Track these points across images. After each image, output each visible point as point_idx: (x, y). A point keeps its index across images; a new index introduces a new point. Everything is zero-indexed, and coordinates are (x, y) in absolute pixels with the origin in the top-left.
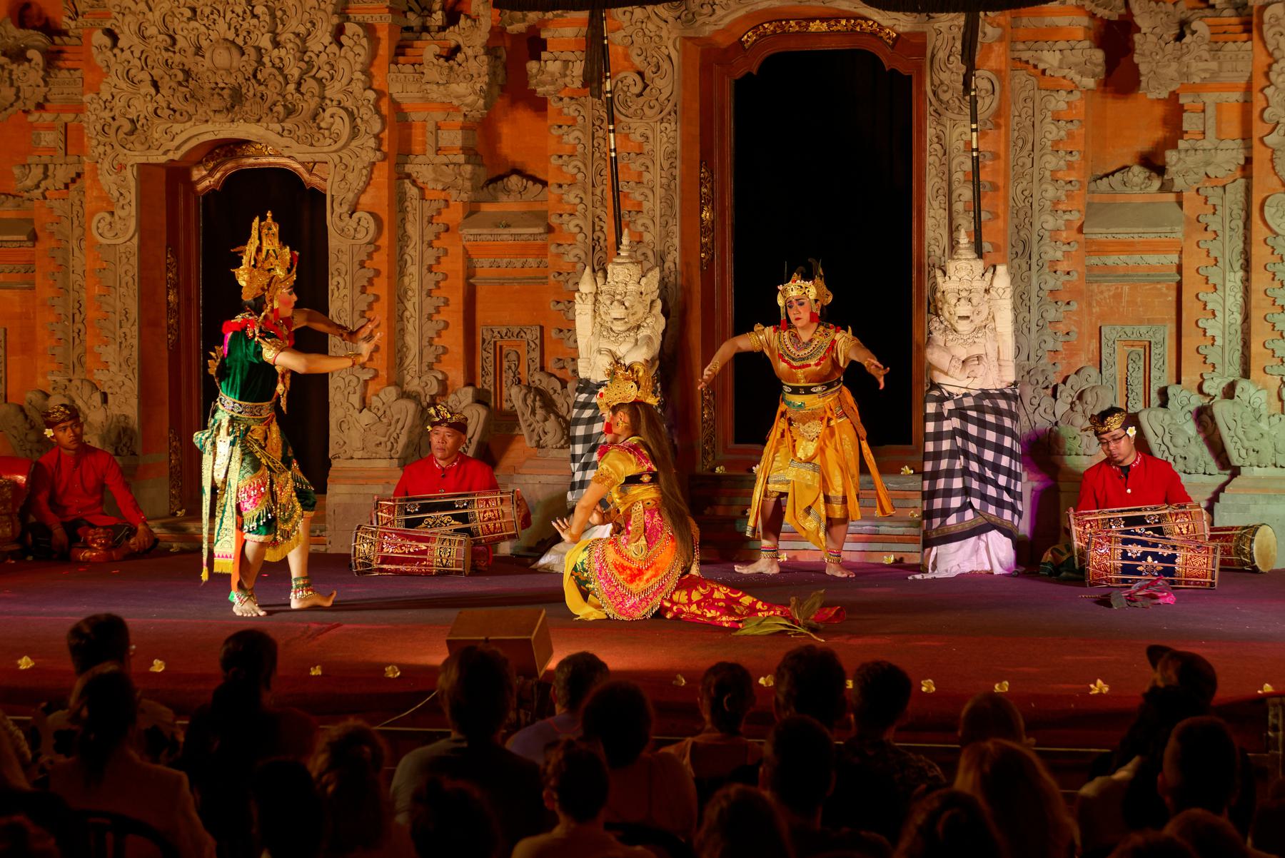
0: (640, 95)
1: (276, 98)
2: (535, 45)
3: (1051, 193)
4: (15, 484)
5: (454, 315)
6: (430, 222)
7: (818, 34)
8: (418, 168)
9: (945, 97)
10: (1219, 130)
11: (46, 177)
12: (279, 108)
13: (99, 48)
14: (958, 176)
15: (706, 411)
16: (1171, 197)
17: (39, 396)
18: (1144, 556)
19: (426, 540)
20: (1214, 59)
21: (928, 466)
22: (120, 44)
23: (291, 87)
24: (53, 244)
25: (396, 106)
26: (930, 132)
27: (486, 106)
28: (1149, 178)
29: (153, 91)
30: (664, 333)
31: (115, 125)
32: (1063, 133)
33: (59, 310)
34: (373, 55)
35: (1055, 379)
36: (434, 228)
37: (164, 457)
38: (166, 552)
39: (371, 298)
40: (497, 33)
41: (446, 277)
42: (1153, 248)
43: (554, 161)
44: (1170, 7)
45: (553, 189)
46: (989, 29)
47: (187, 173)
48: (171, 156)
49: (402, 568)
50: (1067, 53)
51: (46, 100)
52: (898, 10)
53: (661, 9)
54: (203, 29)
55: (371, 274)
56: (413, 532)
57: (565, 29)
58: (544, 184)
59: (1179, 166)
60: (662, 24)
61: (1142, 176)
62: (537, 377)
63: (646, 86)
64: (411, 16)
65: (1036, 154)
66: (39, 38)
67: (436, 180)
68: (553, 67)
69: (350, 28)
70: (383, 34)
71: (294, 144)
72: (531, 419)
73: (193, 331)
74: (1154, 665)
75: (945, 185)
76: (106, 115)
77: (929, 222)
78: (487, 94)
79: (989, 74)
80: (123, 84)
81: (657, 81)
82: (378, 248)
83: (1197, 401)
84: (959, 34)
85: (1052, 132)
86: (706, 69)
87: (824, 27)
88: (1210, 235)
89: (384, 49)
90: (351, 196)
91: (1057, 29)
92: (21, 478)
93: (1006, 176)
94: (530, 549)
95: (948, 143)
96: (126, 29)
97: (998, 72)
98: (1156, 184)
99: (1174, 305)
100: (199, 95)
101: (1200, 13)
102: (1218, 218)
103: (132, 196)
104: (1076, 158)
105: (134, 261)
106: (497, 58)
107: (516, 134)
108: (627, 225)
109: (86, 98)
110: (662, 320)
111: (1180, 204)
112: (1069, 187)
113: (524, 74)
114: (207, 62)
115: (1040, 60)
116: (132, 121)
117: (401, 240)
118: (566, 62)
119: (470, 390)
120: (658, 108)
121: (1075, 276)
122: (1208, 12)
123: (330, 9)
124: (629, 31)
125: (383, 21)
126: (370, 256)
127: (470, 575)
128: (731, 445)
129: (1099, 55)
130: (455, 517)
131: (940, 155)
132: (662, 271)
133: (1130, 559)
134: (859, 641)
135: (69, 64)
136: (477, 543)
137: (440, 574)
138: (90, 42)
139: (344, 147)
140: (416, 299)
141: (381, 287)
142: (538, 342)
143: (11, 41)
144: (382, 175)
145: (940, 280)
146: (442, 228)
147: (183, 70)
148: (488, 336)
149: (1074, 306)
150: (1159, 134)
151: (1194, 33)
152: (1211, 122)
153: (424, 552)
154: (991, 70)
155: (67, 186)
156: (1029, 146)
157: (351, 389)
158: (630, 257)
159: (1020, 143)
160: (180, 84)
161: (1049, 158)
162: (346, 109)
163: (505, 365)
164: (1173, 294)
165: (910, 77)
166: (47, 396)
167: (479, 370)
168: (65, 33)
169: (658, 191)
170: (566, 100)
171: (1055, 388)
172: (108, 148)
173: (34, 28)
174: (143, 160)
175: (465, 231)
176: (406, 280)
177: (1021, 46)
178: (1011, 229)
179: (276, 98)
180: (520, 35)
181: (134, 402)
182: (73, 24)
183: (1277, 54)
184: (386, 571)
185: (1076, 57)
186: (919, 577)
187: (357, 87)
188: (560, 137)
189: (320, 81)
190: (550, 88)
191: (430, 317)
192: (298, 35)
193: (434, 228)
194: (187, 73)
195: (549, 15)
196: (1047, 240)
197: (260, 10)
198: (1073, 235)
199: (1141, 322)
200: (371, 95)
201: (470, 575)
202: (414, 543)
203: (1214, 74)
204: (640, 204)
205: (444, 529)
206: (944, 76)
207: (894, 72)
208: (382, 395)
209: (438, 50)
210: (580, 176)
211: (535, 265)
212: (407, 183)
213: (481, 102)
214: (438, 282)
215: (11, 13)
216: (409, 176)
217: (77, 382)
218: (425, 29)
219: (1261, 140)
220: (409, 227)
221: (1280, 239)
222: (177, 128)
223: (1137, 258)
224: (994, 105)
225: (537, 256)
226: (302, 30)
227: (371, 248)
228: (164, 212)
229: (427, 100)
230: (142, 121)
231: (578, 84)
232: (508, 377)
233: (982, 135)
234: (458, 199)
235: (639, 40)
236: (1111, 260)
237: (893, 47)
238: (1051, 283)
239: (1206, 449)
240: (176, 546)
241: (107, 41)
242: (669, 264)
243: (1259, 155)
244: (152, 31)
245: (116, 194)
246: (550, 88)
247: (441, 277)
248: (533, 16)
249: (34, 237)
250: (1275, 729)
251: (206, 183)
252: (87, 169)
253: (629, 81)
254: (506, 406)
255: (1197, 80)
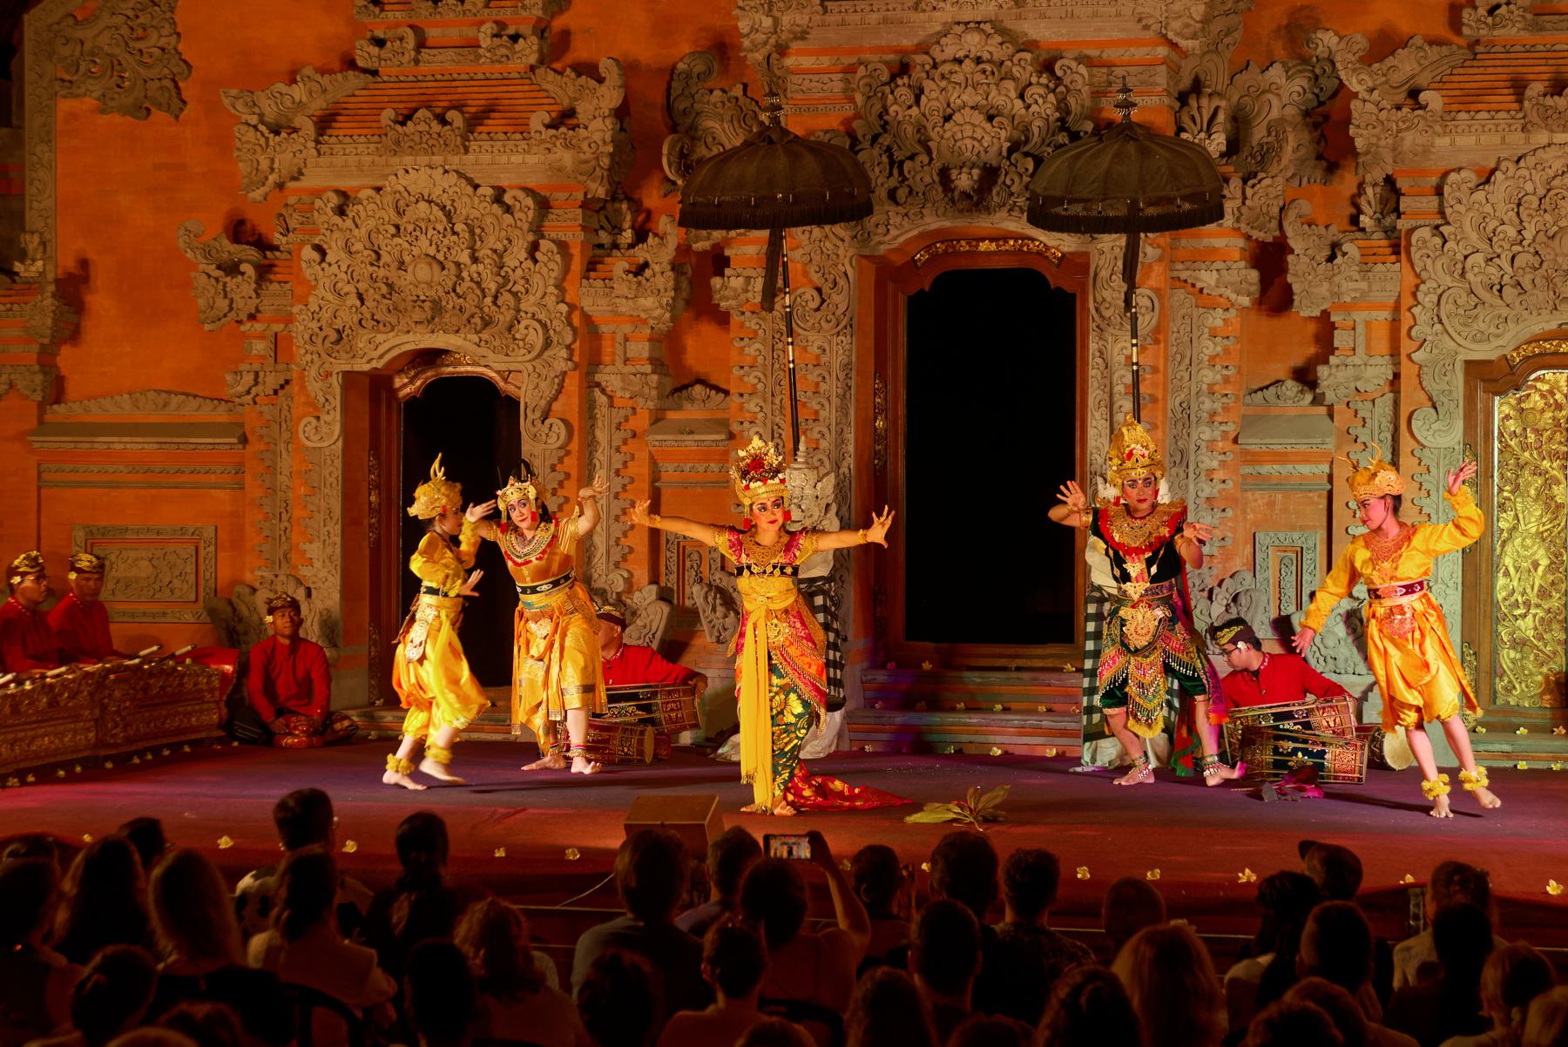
0: (818, 309)
1: (474, 310)
2: (718, 262)
3: (1208, 405)
4: (224, 675)
6: (618, 428)
7: (988, 254)
8: (606, 377)
9: (1107, 314)
10: (1368, 346)
11: (256, 383)
12: (477, 320)
13: (309, 262)
14: (1119, 388)
16: (1323, 410)
17: (247, 590)
18: (1295, 751)
20: (1363, 279)
21: (1088, 664)
22: (328, 259)
23: (488, 300)
24: (262, 447)
25: (587, 319)
26: (1093, 346)
27: (672, 319)
28: (1302, 392)
29: (358, 303)
31: (322, 334)
32: (1219, 349)
33: (267, 509)
34: (566, 270)
35: (1210, 582)
36: (622, 434)
37: (364, 649)
38: (364, 740)
39: (562, 500)
40: (684, 250)
41: (632, 480)
42: (1305, 459)
43: (736, 372)
44: (1322, 230)
45: (735, 398)
46: (1149, 250)
47: (390, 380)
48: (374, 364)
50: (1224, 272)
51: (258, 311)
52: (1061, 230)
53: (839, 229)
54: (406, 245)
55: (561, 477)
57: (748, 247)
58: (727, 393)
59: (1331, 381)
60: (839, 243)
61: (1295, 390)
62: (718, 575)
63: (823, 301)
64: (603, 234)
65: (1194, 369)
66: (251, 253)
67: (624, 389)
68: (737, 283)
69: (545, 245)
70: (576, 251)
71: (489, 353)
72: (712, 616)
73: (394, 530)
74: (1303, 856)
75: (1106, 397)
76: (314, 325)
77: (1091, 432)
78: (672, 308)
79: (1148, 292)
80: (330, 297)
81: (834, 296)
82: (568, 453)
83: (1346, 604)
84: (1119, 253)
85: (1209, 348)
86: (880, 287)
87: (993, 247)
88: (1359, 447)
89: (577, 265)
90: (543, 403)
91: (1215, 250)
92: (228, 668)
93: (1165, 389)
94: (708, 739)
95: (1109, 355)
96: (333, 244)
97: (1157, 291)
98: (1309, 397)
99: (1325, 513)
100: (401, 307)
101: (1351, 236)
102: (1367, 431)
103: (337, 402)
104: (1231, 372)
105: (338, 463)
106: (684, 274)
107: (700, 346)
108: (805, 433)
109: (295, 310)
111: (1331, 416)
112: (1225, 400)
113: (709, 288)
114: (409, 276)
115: (1198, 279)
116: (338, 331)
117: (590, 445)
118: (748, 278)
119: (654, 588)
120: (834, 322)
121: (1230, 484)
122: (1359, 235)
123: (526, 227)
124: (808, 249)
125: (575, 238)
126: (561, 460)
129: (1254, 275)
130: (639, 707)
131: (1102, 367)
132: (837, 476)
133: (1282, 754)
134: (1020, 830)
135: (279, 277)
136: (662, 733)
138: (300, 259)
139: (539, 356)
143: (225, 256)
144: (572, 384)
145: (1101, 487)
146: (630, 434)
147: (387, 284)
149: (1229, 513)
150: (1311, 350)
151: (1344, 254)
152: (1361, 340)
154: (1151, 289)
155: (276, 392)
156: (1187, 361)
158: (806, 462)
159: (1178, 357)
160: (384, 297)
161: (1206, 372)
162: (539, 321)
163: (688, 564)
164: (1324, 502)
165: (1074, 296)
166: (254, 590)
167: (663, 569)
168: (277, 248)
169: (834, 400)
170: (748, 314)
171: (1211, 591)
172: (315, 357)
173: (248, 243)
174: (348, 368)
175: (651, 438)
177: (1180, 266)
178: (1170, 439)
179: (474, 310)
180: (705, 252)
181: (337, 596)
182: (284, 240)
183: (1424, 275)
185: (1233, 276)
186: (1079, 769)
187: (550, 301)
188: (742, 349)
189: (515, 294)
190: (733, 303)
192: (495, 251)
193: (622, 434)
194: (390, 286)
195: (733, 233)
196: (1203, 449)
197: (459, 227)
198: (1228, 445)
199: (1293, 529)
200: (564, 308)
203: (1364, 294)
204: (816, 413)
206: (1107, 294)
207: (1058, 289)
209: (627, 266)
210: (760, 386)
212: (597, 392)
213: (668, 315)
215: (226, 230)
216: (598, 385)
217: (282, 578)
218: (616, 246)
219: (1409, 356)
220: (598, 433)
221: (1426, 452)
222: (380, 338)
223: (1289, 467)
224: (1154, 322)
225: (719, 461)
226: (499, 247)
227: (562, 453)
228: (367, 417)
229: (616, 313)
230: (347, 331)
231: (758, 299)
232: (690, 575)
233: (1143, 350)
234: (646, 406)
235: (817, 258)
236: (1265, 469)
237: (1058, 265)
238: (1207, 490)
239: (1355, 650)
240: (373, 735)
241: (316, 256)
243: (1407, 370)
244: (358, 246)
245: (322, 400)
246: (733, 303)
247: (626, 481)
248: (717, 235)
249: (244, 440)
250: (1416, 918)
251: (408, 390)
252: (295, 376)
253: (808, 296)
254: (688, 603)
255: (1348, 299)
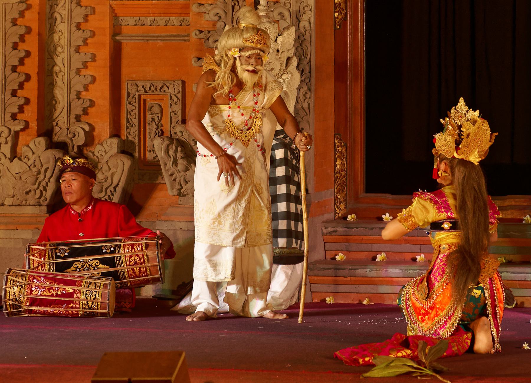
5: (101, 71)
15: (338, 162)
19: (72, 283)
30: (299, 89)
39: (23, 54)
41: (93, 34)
49: (50, 310)
55: (22, 31)
56: (61, 275)
72: (173, 169)
110: (297, 77)
119: (115, 141)
126: (22, 14)
127: (115, 316)
128: (363, 195)
132: (298, 30)
136: (124, 286)
137: (86, 315)
140: (65, 55)
141: (32, 44)
142: (180, 96)
148: (132, 91)
153: (71, 295)
157: (3, 140)
158: (267, 16)
163: (149, 117)
167: (124, 122)
176: (56, 37)
184: (35, 312)
191: (78, 72)
201: (115, 316)
202: (61, 286)
205: (92, 272)
208: (32, 145)
211: (177, 24)
214: (86, 39)
232: (151, 128)
242: (304, 23)
247: (88, 34)
254: (149, 156)
